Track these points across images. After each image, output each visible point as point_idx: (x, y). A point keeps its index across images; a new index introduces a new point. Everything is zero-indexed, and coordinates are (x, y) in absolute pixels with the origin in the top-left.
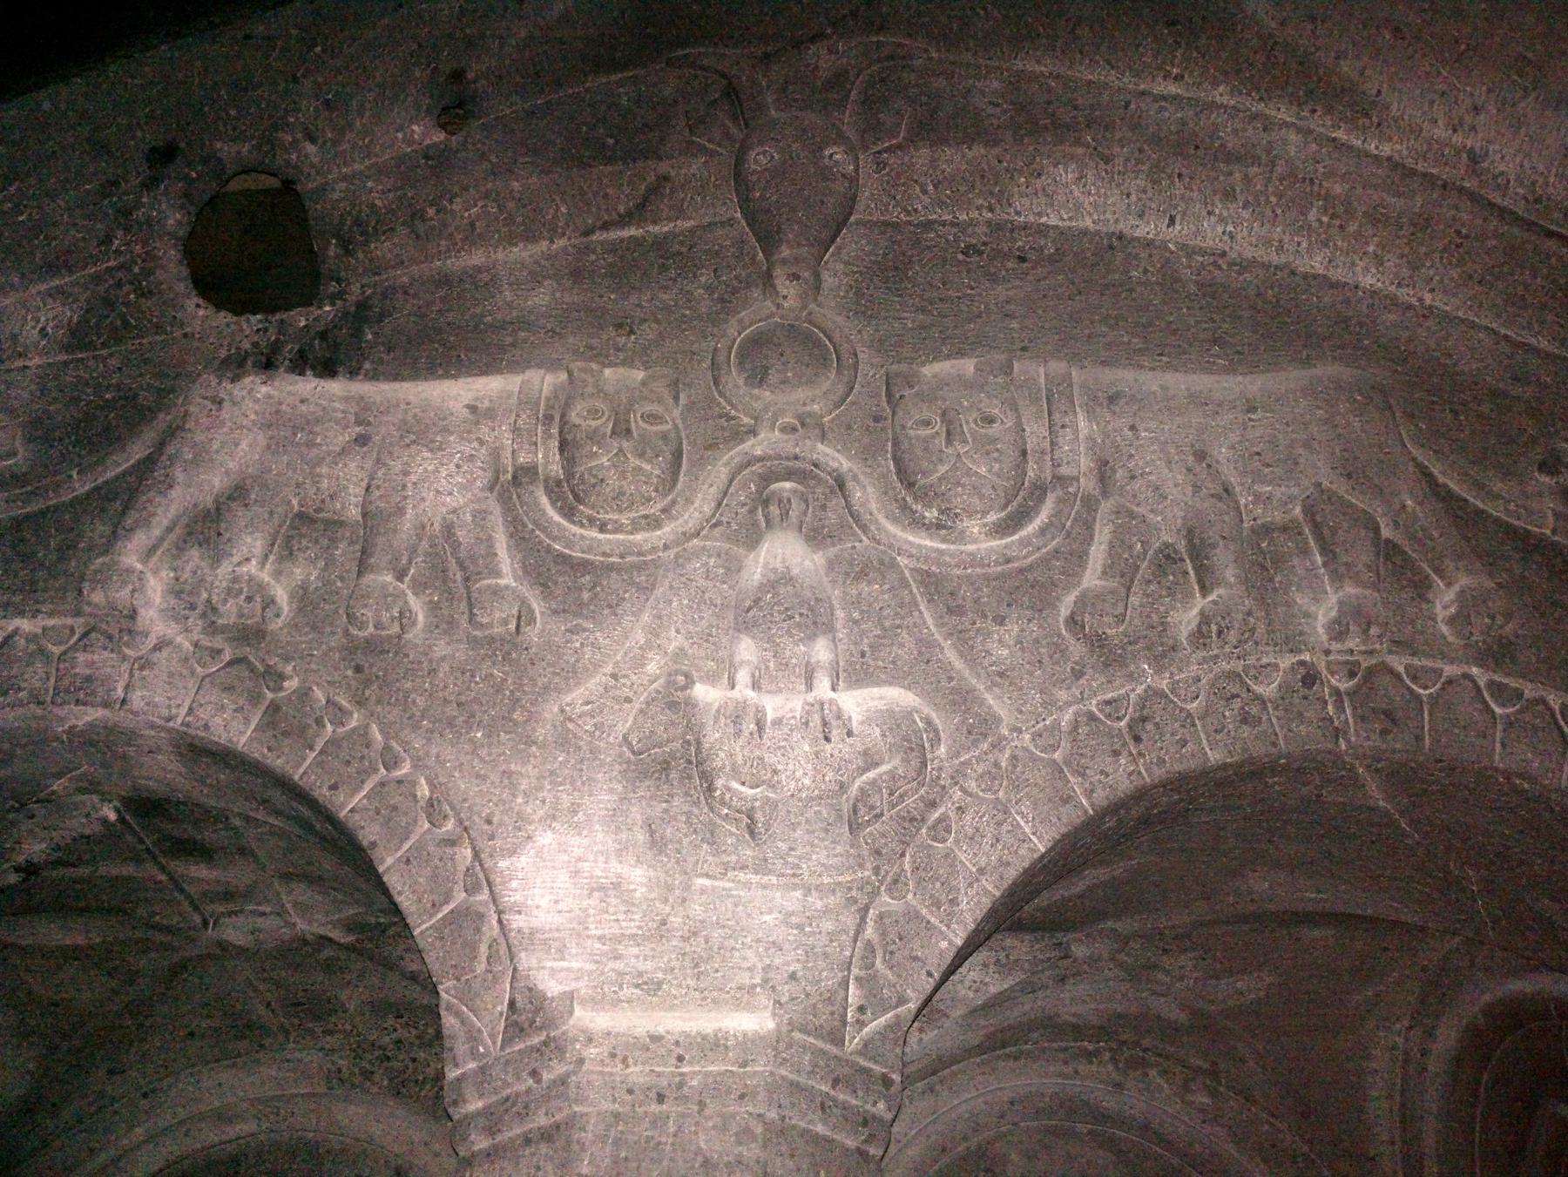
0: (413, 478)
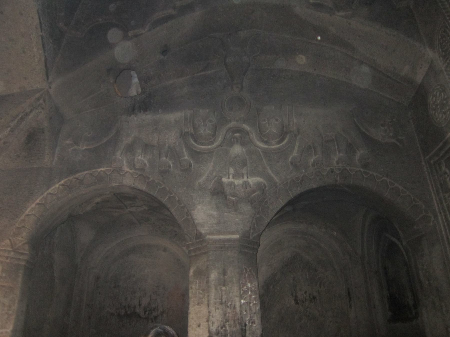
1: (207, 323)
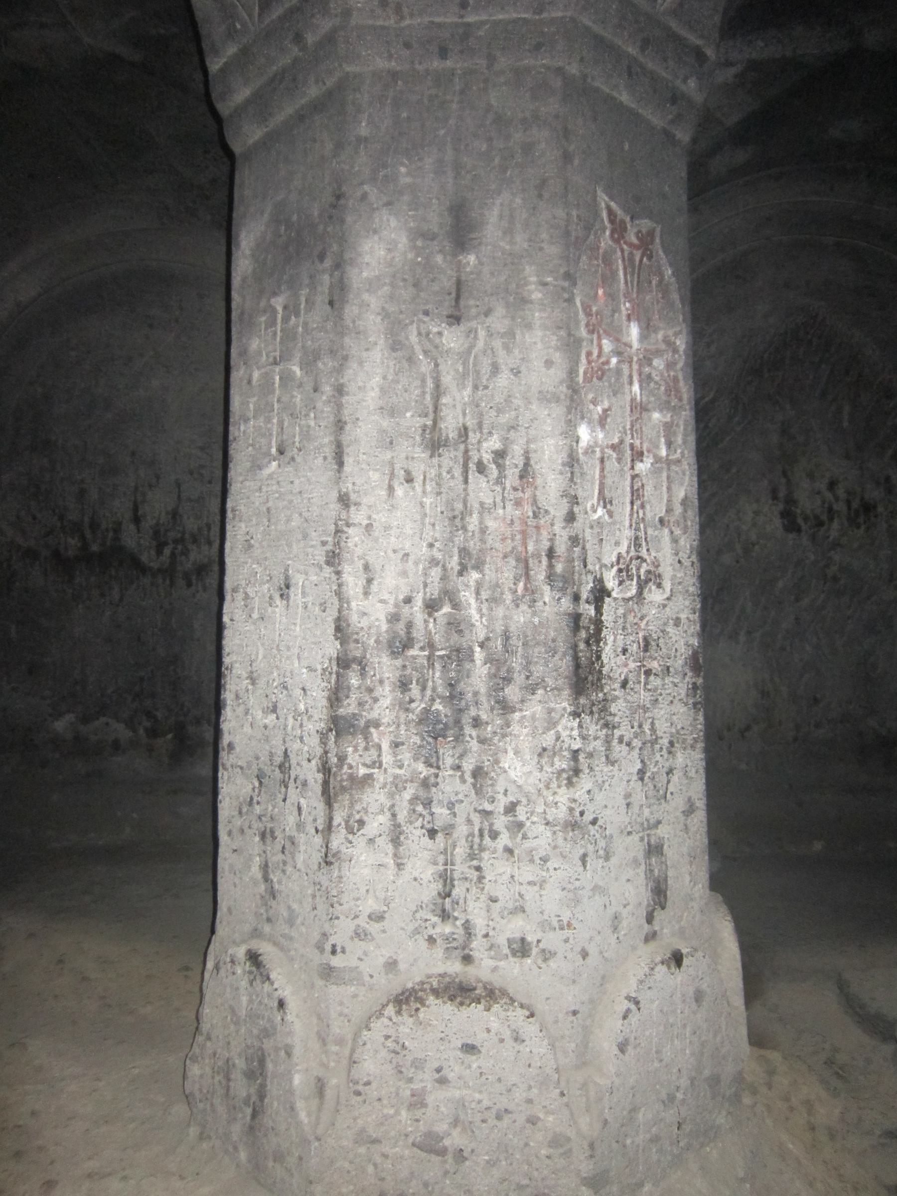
1: (328, 571)
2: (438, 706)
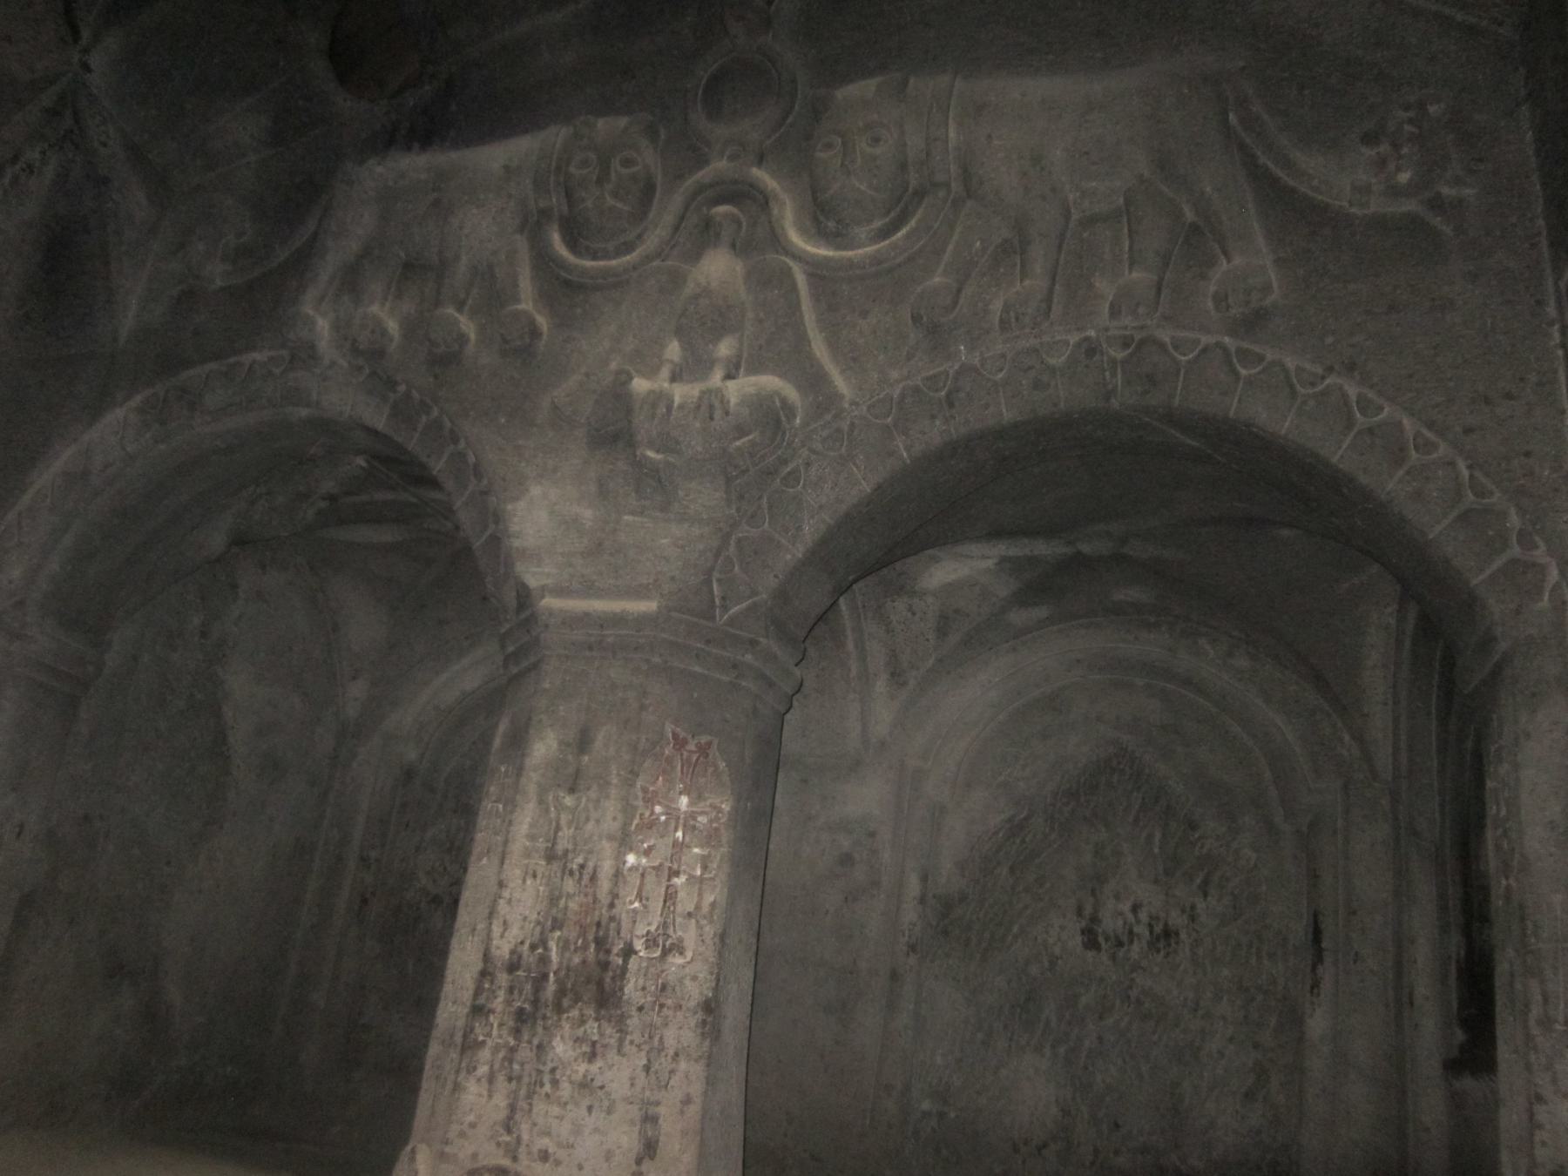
0: (466, 231)
2: (526, 1006)
